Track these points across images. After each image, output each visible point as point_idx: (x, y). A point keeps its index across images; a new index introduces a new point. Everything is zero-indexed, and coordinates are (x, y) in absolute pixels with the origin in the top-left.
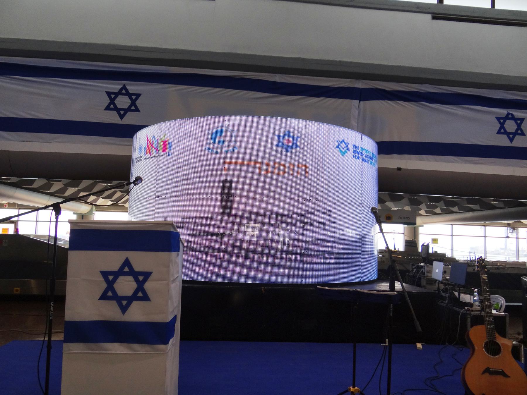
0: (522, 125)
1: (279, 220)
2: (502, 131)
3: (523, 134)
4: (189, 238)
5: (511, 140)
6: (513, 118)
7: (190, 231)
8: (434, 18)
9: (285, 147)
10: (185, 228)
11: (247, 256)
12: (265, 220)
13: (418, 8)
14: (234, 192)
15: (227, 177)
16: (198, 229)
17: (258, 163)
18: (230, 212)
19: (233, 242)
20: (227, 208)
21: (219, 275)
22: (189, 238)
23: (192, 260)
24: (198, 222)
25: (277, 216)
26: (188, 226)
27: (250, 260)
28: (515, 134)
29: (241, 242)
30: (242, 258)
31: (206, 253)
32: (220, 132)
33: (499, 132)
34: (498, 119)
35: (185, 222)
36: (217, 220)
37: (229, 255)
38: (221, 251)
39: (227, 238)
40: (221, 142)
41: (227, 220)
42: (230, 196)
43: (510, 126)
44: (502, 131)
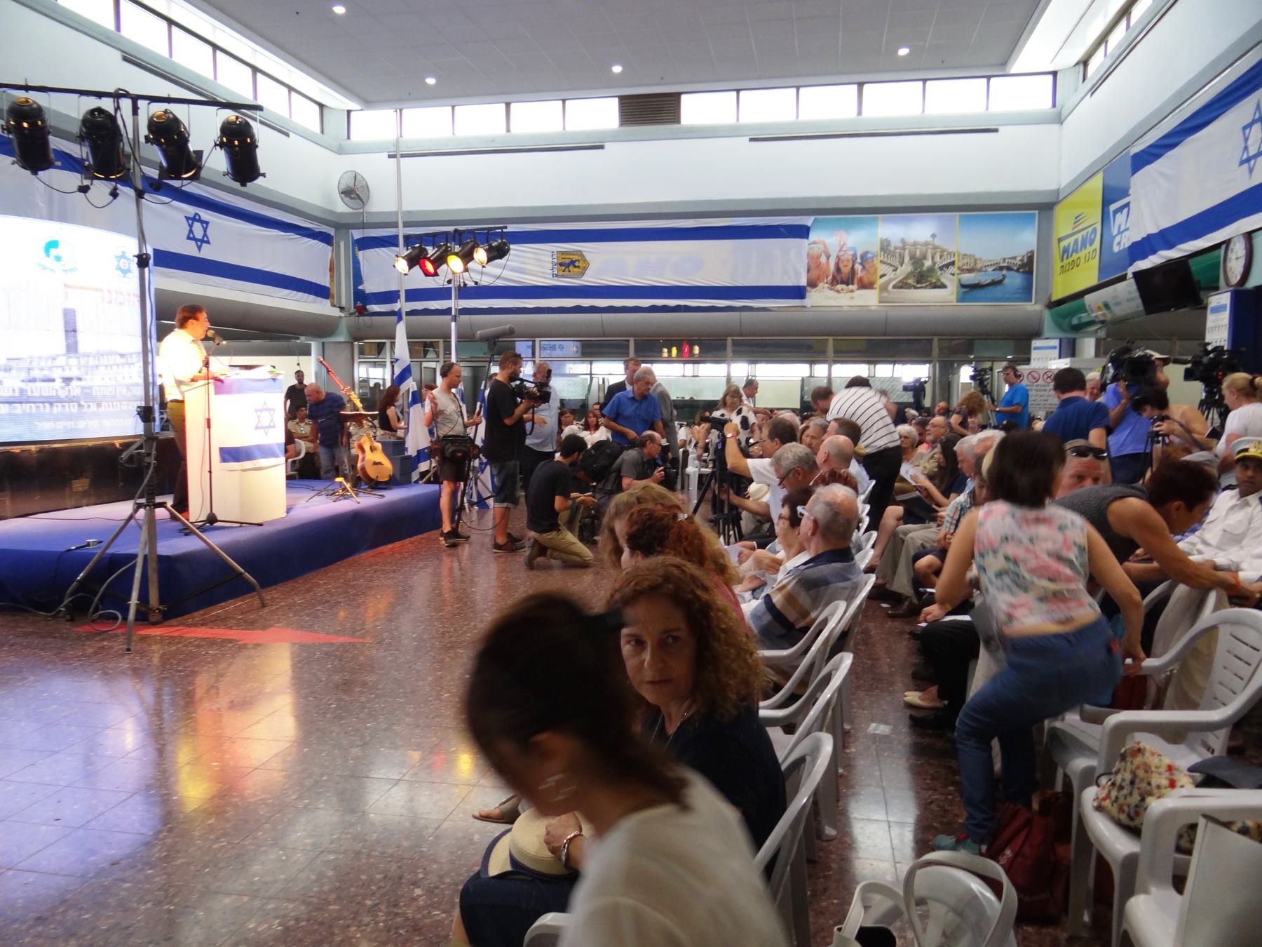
0: (208, 230)
1: (124, 360)
2: (191, 237)
3: (208, 242)
4: (24, 385)
5: (199, 248)
6: (200, 221)
7: (23, 375)
8: (125, 59)
9: (122, 271)
10: (14, 372)
11: (99, 405)
12: (111, 362)
13: (108, 37)
14: (80, 326)
15: (70, 306)
16: (36, 373)
17: (101, 290)
18: (76, 351)
19: (83, 388)
20: (72, 348)
21: (71, 430)
22: (24, 385)
23: (30, 414)
24: (35, 364)
25: (122, 356)
26: (20, 369)
27: (102, 409)
28: (202, 241)
29: (90, 388)
30: (93, 407)
31: (51, 404)
32: (53, 244)
33: (189, 238)
34: (187, 218)
35: (13, 364)
36: (61, 361)
37: (80, 405)
38: (70, 400)
39: (74, 383)
40: (58, 258)
41: (73, 361)
42: (75, 331)
43: (198, 230)
44: (191, 237)
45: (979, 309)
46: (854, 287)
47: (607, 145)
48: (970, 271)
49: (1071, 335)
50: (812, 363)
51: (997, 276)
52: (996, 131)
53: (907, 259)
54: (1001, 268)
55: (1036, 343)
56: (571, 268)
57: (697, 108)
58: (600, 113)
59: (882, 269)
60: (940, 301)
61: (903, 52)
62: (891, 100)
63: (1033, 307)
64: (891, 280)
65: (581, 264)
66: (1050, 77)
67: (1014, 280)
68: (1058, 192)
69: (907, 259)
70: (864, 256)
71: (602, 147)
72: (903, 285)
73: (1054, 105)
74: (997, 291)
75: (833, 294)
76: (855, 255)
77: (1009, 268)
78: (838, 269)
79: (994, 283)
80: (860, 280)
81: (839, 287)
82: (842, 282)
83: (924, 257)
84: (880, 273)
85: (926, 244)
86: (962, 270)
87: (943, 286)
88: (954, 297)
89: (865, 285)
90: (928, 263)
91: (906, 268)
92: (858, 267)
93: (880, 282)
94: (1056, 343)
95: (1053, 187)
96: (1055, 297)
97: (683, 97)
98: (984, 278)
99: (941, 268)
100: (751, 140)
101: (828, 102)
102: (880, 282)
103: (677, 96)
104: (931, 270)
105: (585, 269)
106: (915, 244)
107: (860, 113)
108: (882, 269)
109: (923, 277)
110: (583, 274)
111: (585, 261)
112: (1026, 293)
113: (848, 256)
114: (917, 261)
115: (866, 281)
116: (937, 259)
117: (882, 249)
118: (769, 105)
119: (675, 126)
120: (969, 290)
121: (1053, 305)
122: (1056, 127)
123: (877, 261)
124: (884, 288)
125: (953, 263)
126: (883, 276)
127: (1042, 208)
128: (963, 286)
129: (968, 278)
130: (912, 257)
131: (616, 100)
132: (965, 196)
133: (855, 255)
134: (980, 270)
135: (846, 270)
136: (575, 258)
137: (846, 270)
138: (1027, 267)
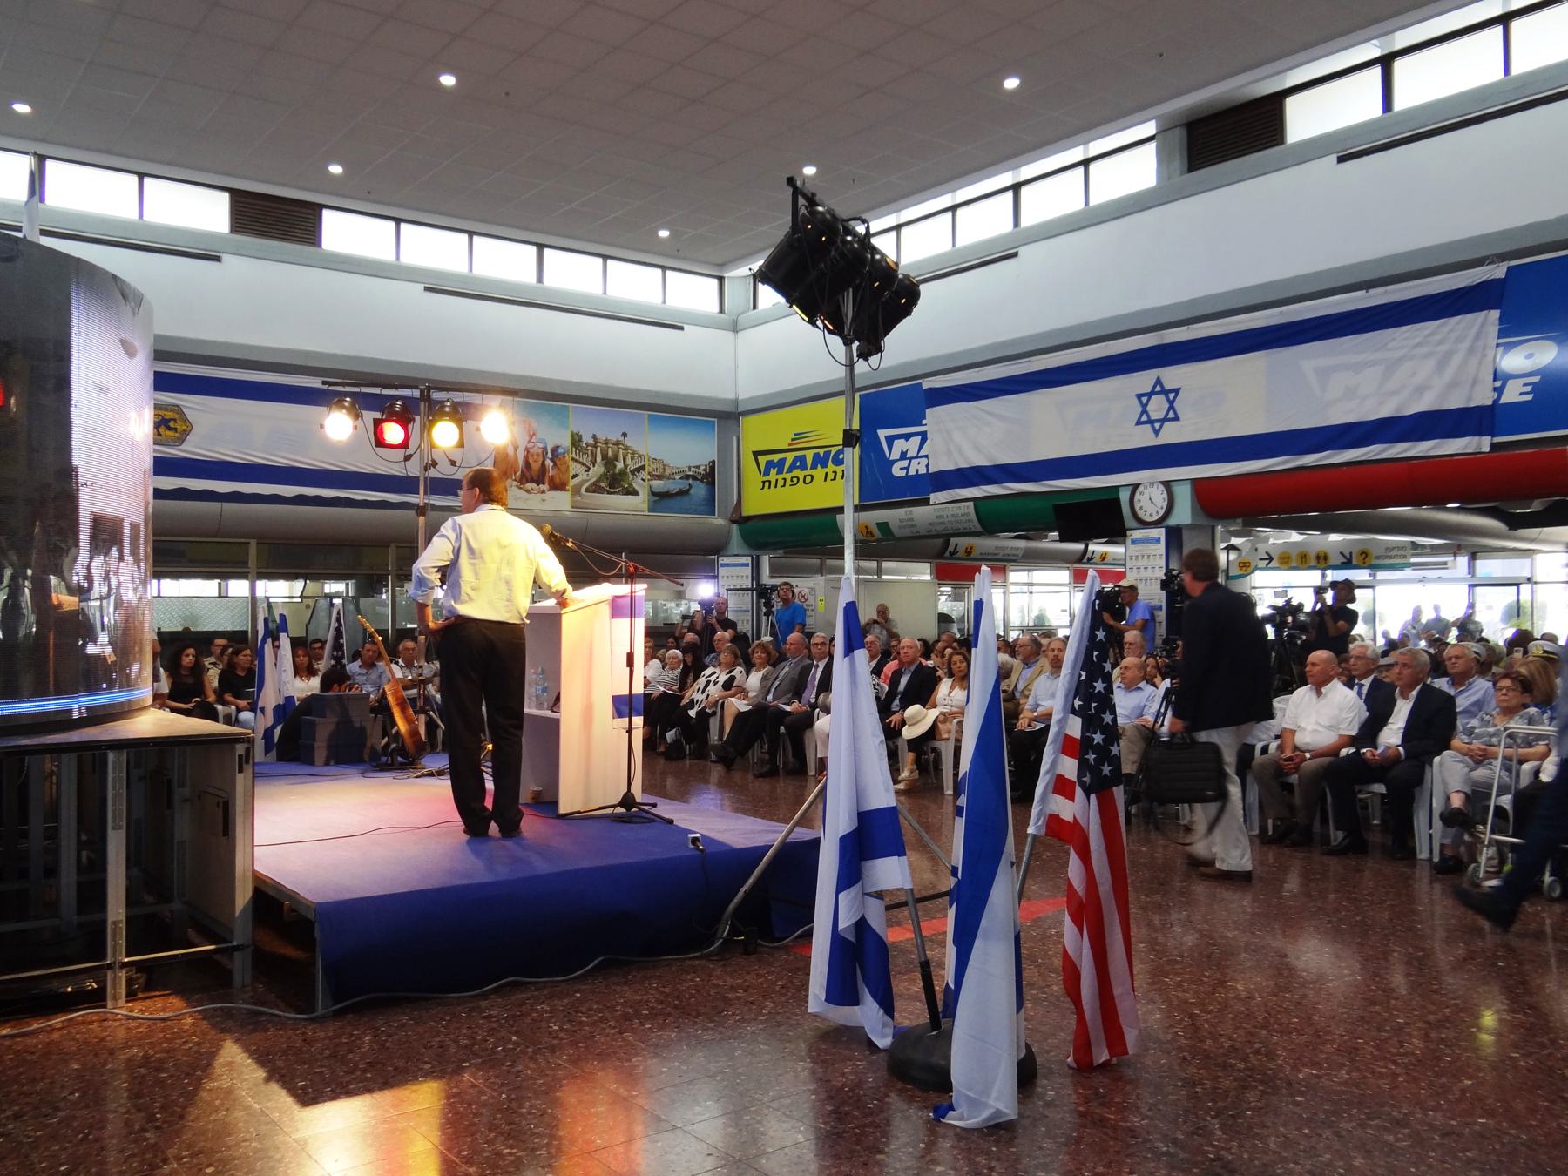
45: (669, 520)
46: (545, 487)
47: (225, 257)
48: (659, 477)
49: (755, 553)
50: (225, 576)
51: (684, 485)
52: (681, 328)
53: (599, 459)
54: (687, 477)
55: (723, 560)
56: (162, 430)
57: (343, 231)
58: (203, 210)
59: (574, 468)
60: (629, 509)
61: (664, 234)
62: (572, 272)
63: (717, 521)
64: (584, 482)
65: (180, 426)
66: (715, 282)
67: (699, 490)
68: (736, 401)
69: (599, 459)
70: (554, 450)
71: (218, 259)
72: (595, 488)
73: (722, 311)
74: (686, 499)
75: (522, 494)
76: (545, 449)
77: (694, 478)
78: (527, 464)
79: (683, 493)
80: (552, 479)
81: (529, 486)
82: (532, 481)
83: (616, 459)
84: (572, 473)
85: (617, 443)
86: (653, 476)
87: (635, 493)
88: (646, 506)
89: (558, 486)
90: (620, 465)
91: (598, 470)
92: (549, 463)
93: (573, 482)
94: (748, 560)
95: (731, 396)
96: (745, 513)
97: (326, 213)
98: (673, 487)
99: (633, 472)
100: (427, 289)
101: (504, 260)
102: (573, 482)
103: (317, 208)
104: (623, 473)
105: (186, 433)
106: (607, 442)
107: (540, 280)
108: (574, 468)
109: (615, 482)
110: (181, 441)
111: (185, 420)
112: (709, 506)
113: (537, 449)
114: (609, 462)
115: (557, 480)
116: (629, 462)
117: (573, 444)
118: (435, 248)
119: (312, 249)
120: (660, 499)
121: (741, 520)
122: (731, 334)
123: (568, 458)
124: (576, 491)
125: (643, 468)
126: (575, 476)
127: (725, 418)
128: (653, 494)
129: (658, 485)
130: (604, 457)
131: (225, 198)
132: (657, 394)
133: (545, 449)
134: (669, 478)
135: (536, 466)
136: (169, 415)
137: (536, 466)
138: (709, 476)
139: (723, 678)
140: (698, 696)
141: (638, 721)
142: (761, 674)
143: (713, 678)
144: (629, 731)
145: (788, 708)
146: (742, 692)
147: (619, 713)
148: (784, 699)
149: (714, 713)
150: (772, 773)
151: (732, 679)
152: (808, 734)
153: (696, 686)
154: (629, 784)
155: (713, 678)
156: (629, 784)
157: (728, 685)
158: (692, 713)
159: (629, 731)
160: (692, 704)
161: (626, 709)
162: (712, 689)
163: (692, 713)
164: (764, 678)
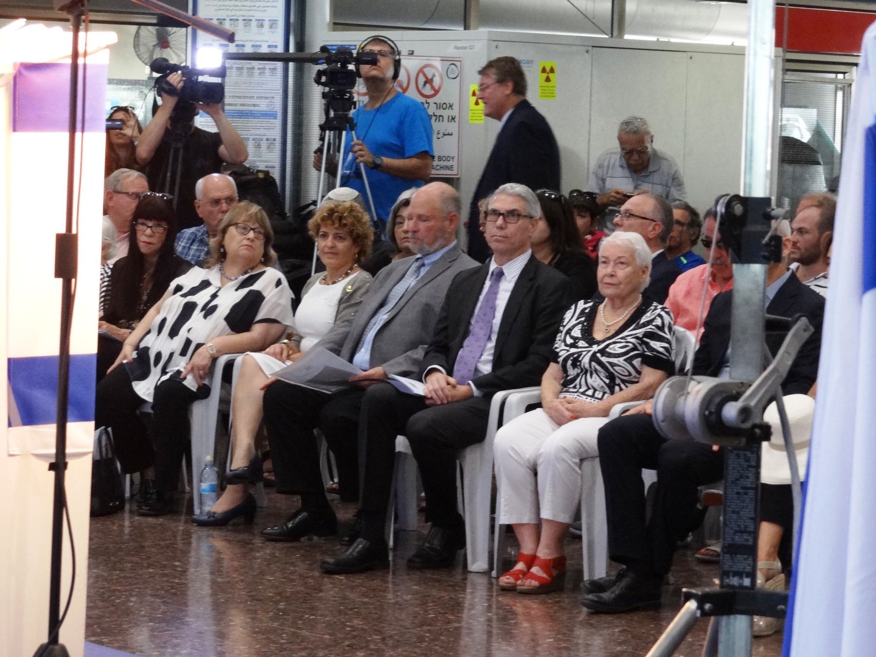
139: (230, 297)
140: (160, 344)
141: (83, 436)
142: (336, 290)
143: (201, 298)
144: (59, 466)
145: (417, 388)
146: (284, 336)
147: (27, 413)
148: (400, 362)
149: (204, 392)
150: (373, 562)
151: (254, 300)
152: (472, 462)
153: (153, 317)
154: (55, 622)
155: (201, 298)
156: (55, 622)
157: (242, 317)
158: (144, 389)
159: (59, 466)
160: (143, 364)
161: (48, 401)
162: (199, 327)
163: (144, 389)
164: (346, 301)
